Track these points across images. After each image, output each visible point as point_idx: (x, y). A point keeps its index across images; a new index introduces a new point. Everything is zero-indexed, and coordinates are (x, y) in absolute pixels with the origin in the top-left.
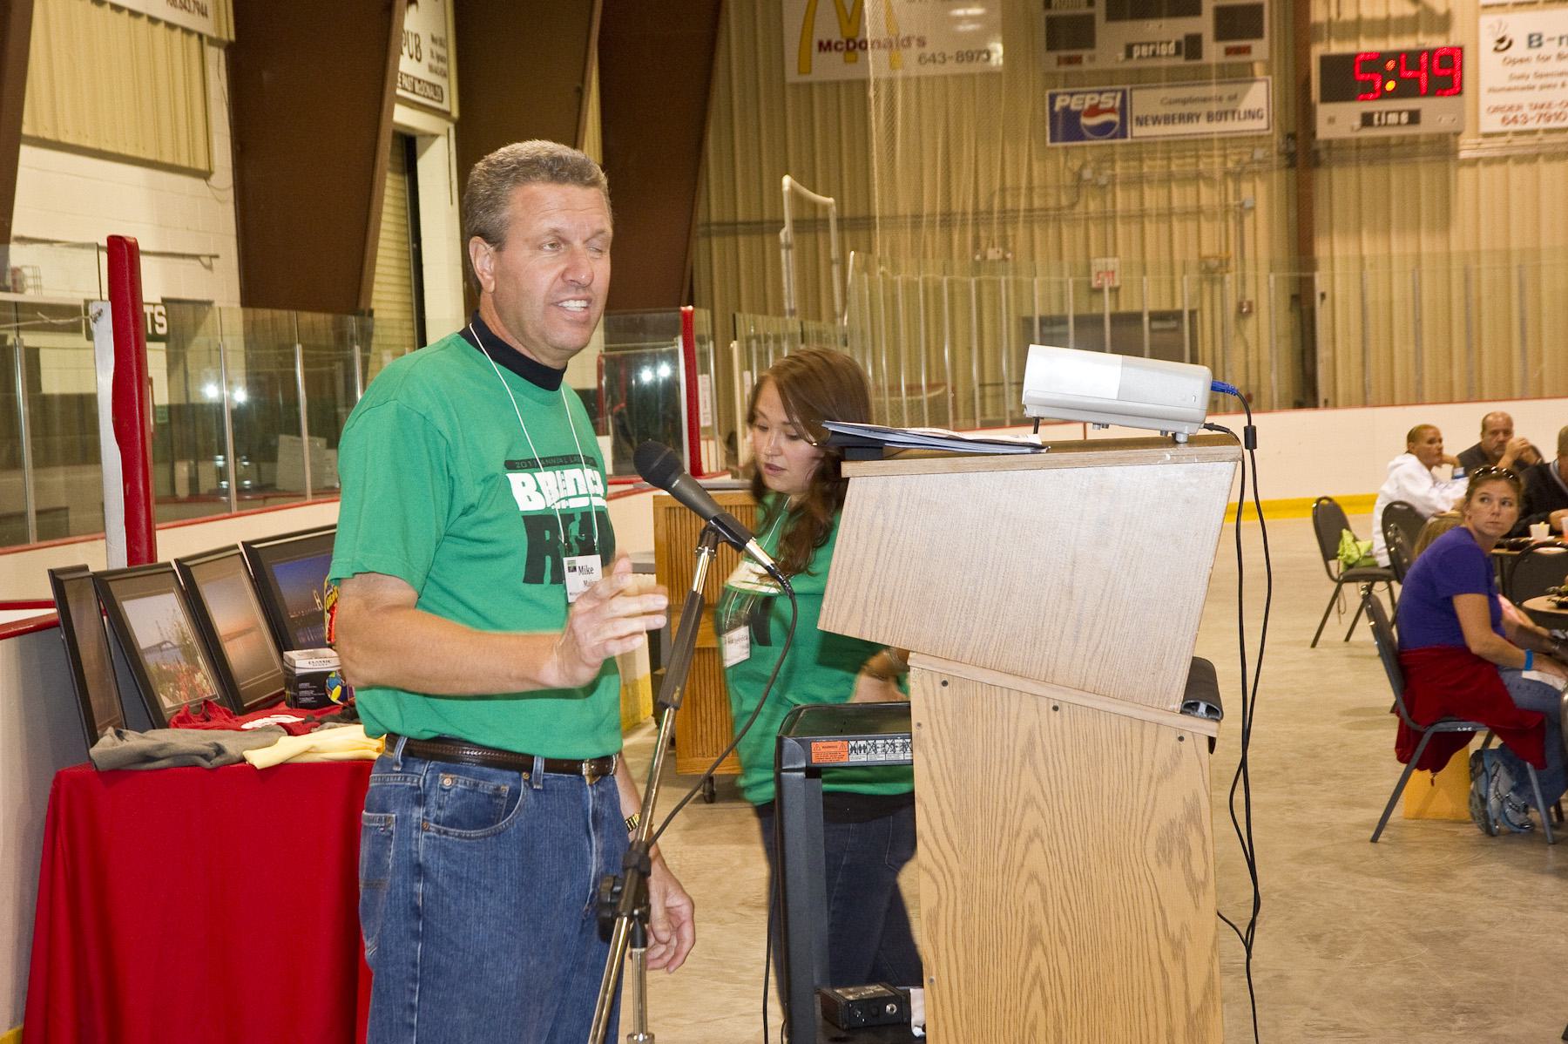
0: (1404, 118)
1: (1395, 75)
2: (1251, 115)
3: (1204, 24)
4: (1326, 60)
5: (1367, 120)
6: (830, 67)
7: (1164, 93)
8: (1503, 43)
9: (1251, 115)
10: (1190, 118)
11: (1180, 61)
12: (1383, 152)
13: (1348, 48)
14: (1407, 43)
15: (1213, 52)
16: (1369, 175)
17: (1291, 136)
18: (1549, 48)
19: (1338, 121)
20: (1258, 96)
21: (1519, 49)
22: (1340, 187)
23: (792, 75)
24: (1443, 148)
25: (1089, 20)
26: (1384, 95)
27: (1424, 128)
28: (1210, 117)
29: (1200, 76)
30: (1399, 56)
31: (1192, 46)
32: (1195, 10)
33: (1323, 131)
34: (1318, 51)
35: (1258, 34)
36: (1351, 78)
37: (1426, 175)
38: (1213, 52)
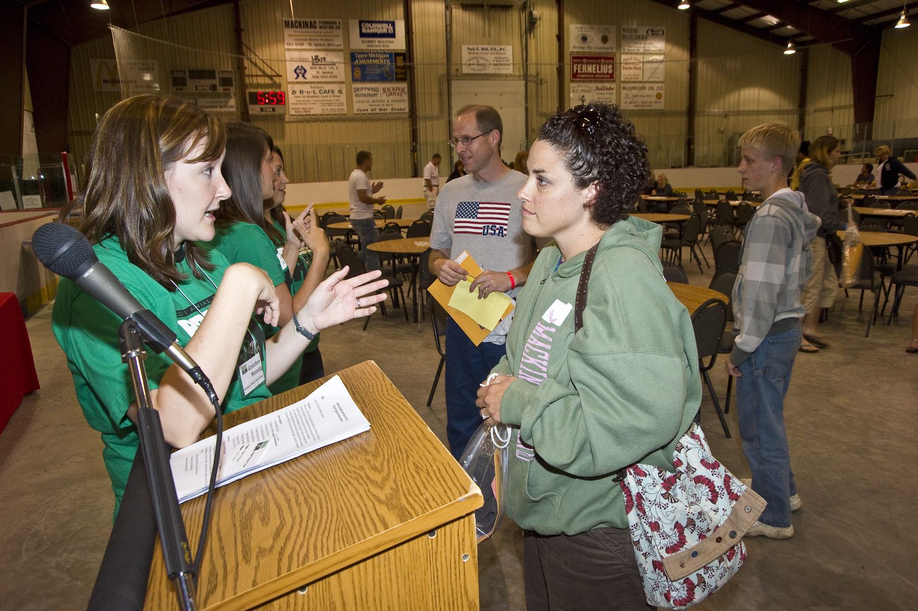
2: (231, 107)
3: (216, 82)
4: (251, 94)
5: (262, 110)
6: (107, 87)
7: (209, 100)
9: (231, 107)
10: (215, 107)
11: (211, 91)
13: (256, 91)
14: (270, 90)
15: (220, 89)
17: (242, 113)
18: (305, 94)
19: (254, 109)
20: (232, 102)
21: (298, 94)
23: (95, 89)
24: (281, 118)
25: (184, 79)
27: (277, 112)
28: (221, 107)
29: (218, 95)
30: (268, 93)
31: (214, 87)
32: (214, 78)
33: (251, 112)
34: (248, 91)
35: (232, 85)
36: (256, 99)
38: (220, 89)
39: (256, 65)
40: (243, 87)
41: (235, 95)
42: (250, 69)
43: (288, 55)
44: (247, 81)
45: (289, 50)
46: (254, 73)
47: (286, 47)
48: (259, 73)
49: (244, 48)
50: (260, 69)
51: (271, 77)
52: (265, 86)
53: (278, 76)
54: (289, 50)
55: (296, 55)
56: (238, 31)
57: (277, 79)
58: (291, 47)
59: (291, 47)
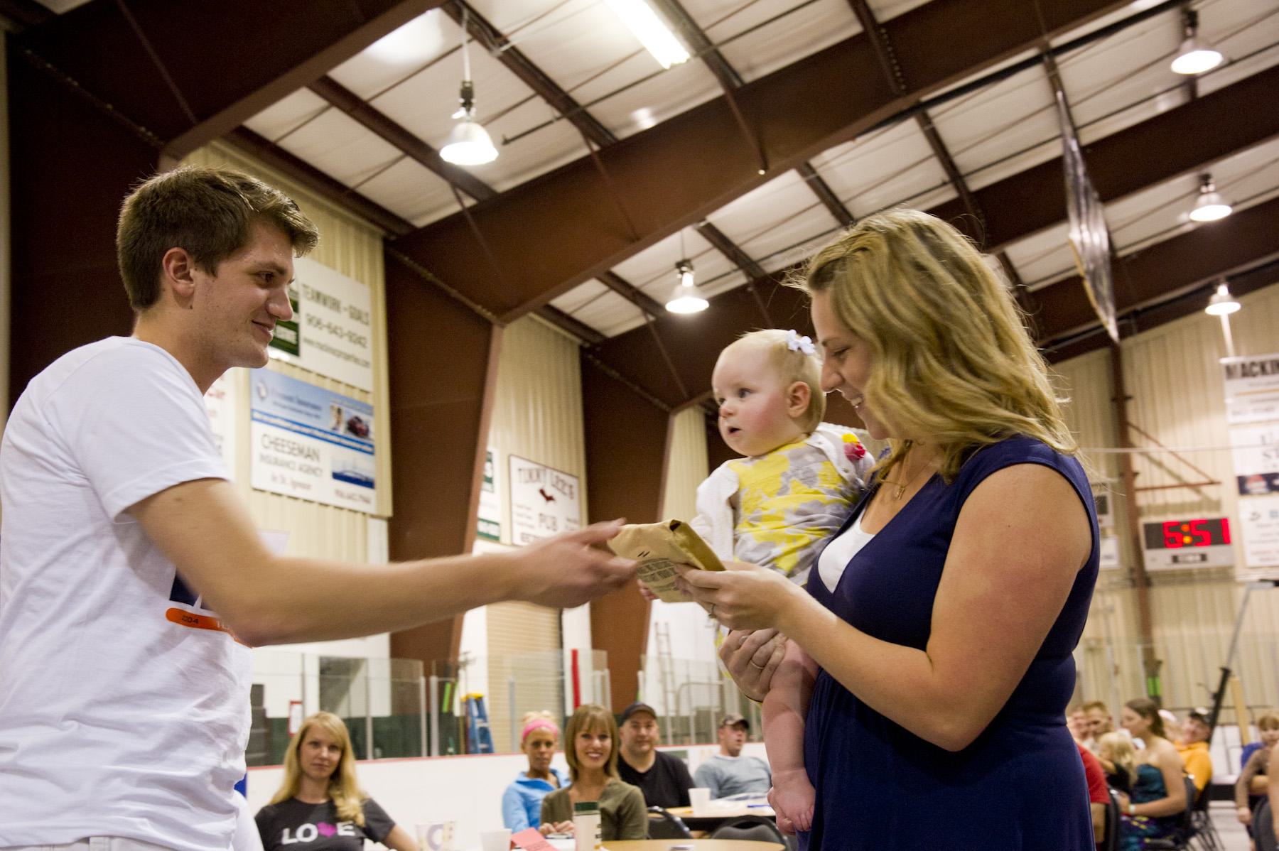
0: (1198, 558)
1: (1191, 534)
4: (1149, 527)
5: (1175, 559)
8: (1255, 516)
12: (1187, 578)
14: (1196, 516)
16: (1183, 592)
19: (1157, 560)
22: (1162, 596)
24: (1224, 576)
26: (1183, 545)
30: (1193, 524)
34: (1143, 520)
37: (1218, 591)
39: (1160, 465)
40: (1134, 512)
41: (1116, 529)
42: (1146, 474)
43: (1236, 437)
44: (1142, 500)
45: (1236, 425)
46: (1157, 483)
47: (1232, 419)
48: (1169, 481)
49: (1134, 436)
50: (1171, 473)
51: (1195, 487)
52: (1182, 508)
53: (1212, 483)
54: (1236, 425)
55: (1253, 435)
56: (1119, 399)
57: (1210, 491)
58: (1239, 419)
59: (1239, 419)
